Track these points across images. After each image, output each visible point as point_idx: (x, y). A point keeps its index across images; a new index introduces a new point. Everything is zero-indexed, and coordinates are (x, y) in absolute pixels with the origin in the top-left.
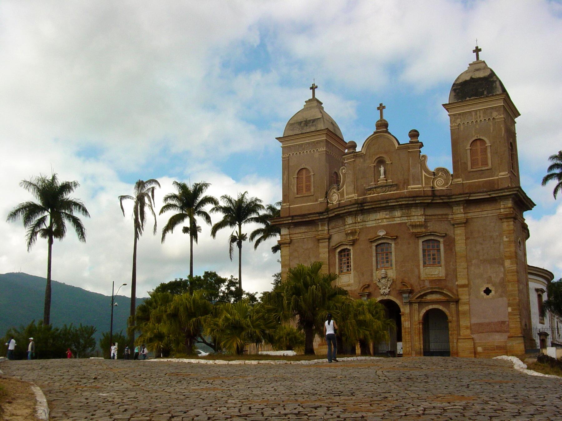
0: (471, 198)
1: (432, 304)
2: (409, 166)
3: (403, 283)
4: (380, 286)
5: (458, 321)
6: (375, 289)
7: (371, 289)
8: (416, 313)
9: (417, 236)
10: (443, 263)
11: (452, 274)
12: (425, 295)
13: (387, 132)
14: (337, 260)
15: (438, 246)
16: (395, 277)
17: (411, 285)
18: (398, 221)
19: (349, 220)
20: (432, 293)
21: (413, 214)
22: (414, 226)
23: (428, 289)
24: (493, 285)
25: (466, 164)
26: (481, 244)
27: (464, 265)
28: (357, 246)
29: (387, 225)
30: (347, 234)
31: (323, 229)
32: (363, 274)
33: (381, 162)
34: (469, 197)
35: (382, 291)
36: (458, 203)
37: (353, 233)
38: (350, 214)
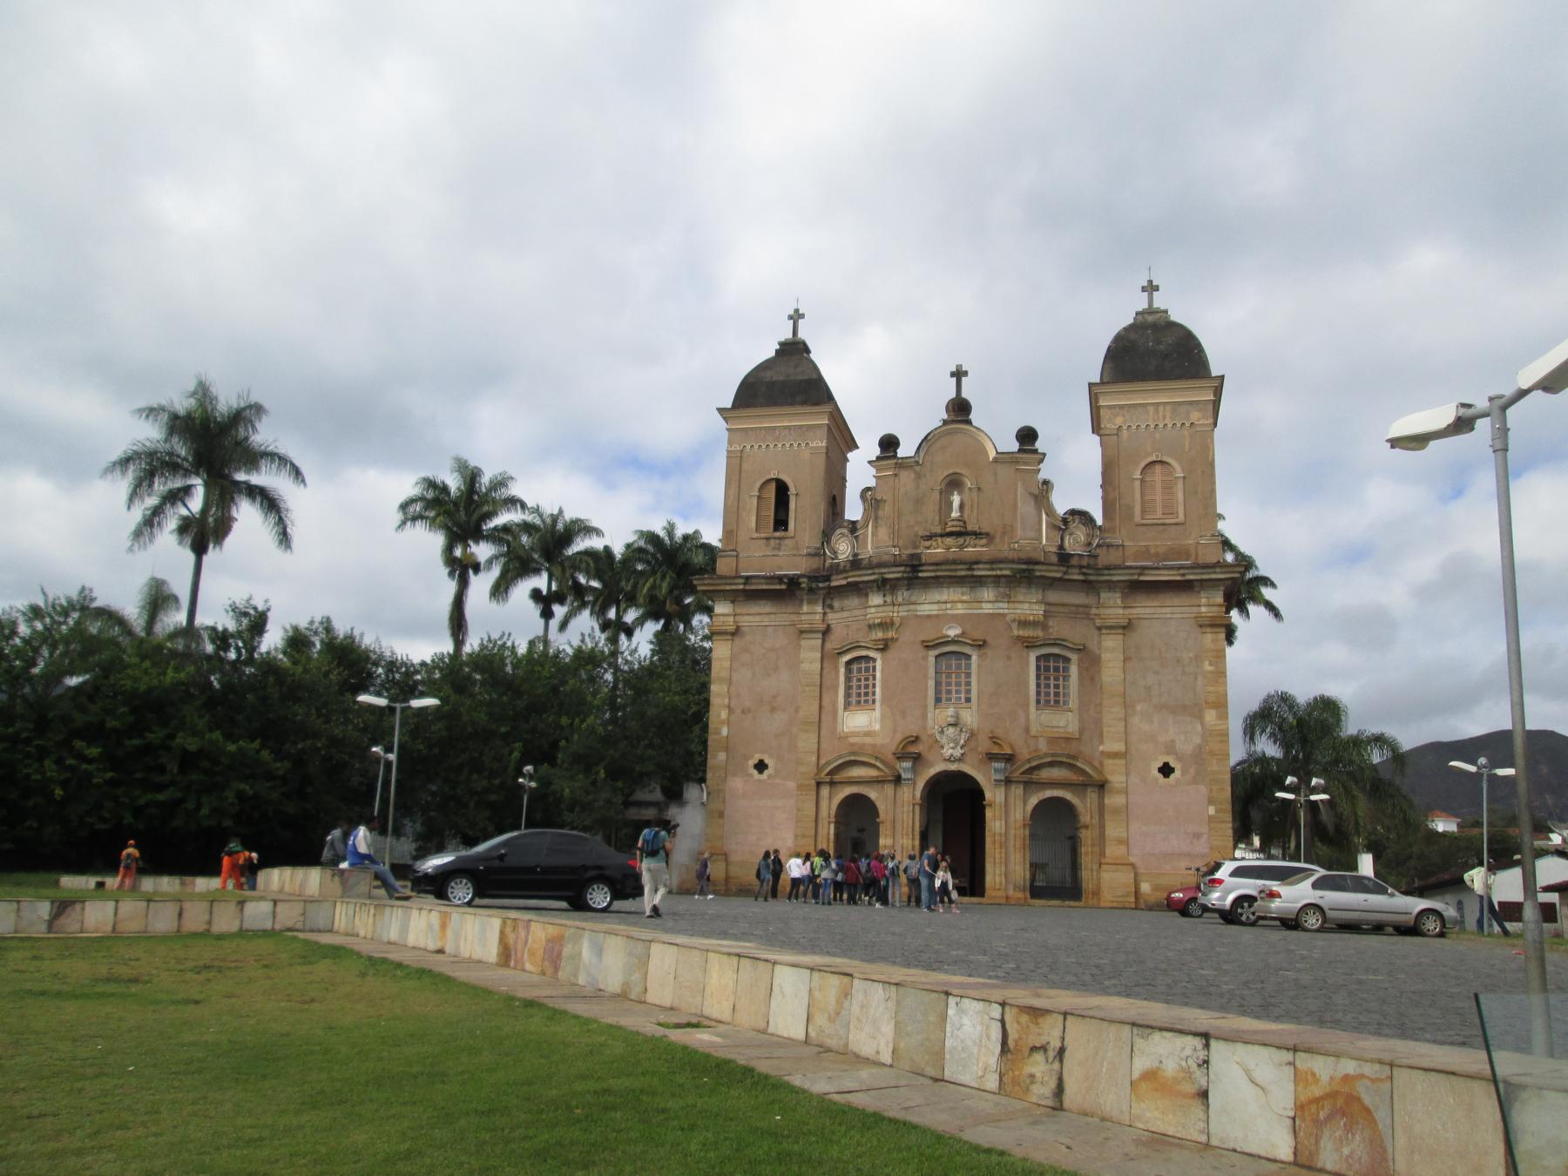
2: (1015, 500)
3: (994, 739)
4: (944, 741)
5: (1102, 826)
6: (931, 747)
8: (1020, 804)
9: (1030, 644)
10: (1073, 702)
11: (1092, 727)
12: (1038, 767)
13: (969, 422)
14: (842, 678)
15: (1066, 669)
16: (975, 726)
17: (1012, 747)
18: (987, 608)
19: (876, 599)
20: (1051, 764)
21: (1021, 598)
22: (1024, 624)
23: (1046, 755)
24: (1179, 759)
25: (1130, 508)
26: (1157, 673)
27: (1118, 711)
28: (892, 653)
29: (963, 615)
30: (871, 627)
31: (812, 612)
32: (904, 714)
33: (954, 483)
35: (947, 752)
36: (1111, 586)
37: (885, 625)
38: (884, 585)
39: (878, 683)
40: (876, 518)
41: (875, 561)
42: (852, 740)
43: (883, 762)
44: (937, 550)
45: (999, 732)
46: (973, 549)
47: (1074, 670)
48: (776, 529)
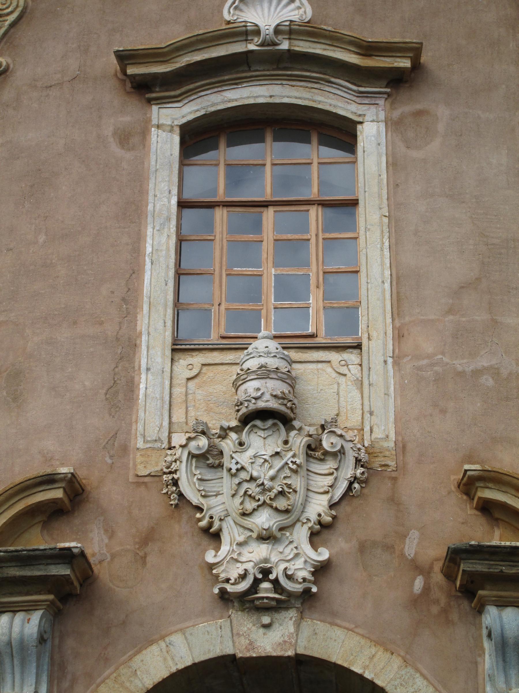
7: (89, 537)
16: (383, 430)
35: (238, 558)
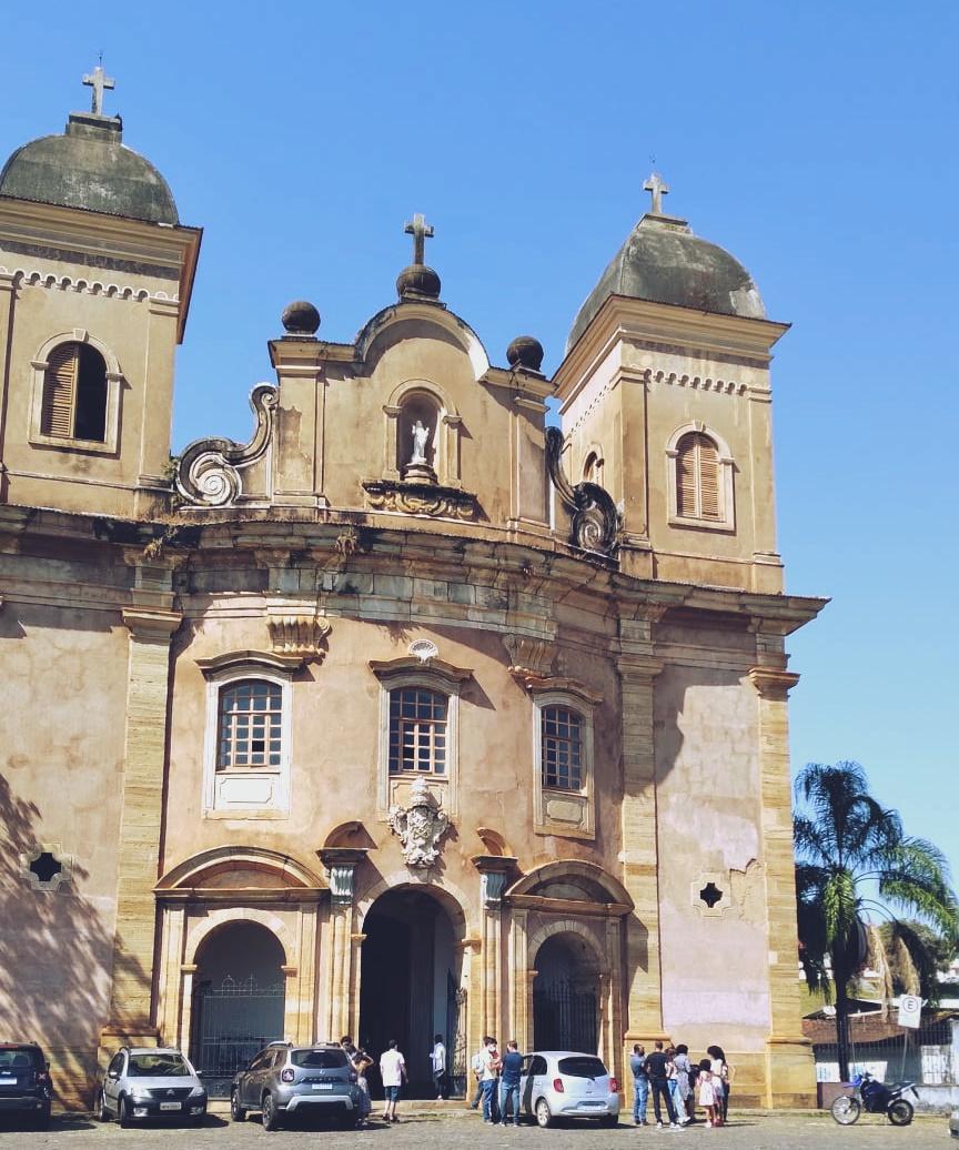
0: (689, 603)
1: (564, 919)
3: (491, 839)
15: (576, 732)
32: (335, 784)
34: (686, 598)
37: (297, 631)
39: (285, 726)
40: (282, 443)
41: (283, 516)
42: (232, 825)
43: (299, 866)
44: (393, 516)
45: (491, 824)
46: (453, 524)
47: (588, 734)
48: (81, 433)
